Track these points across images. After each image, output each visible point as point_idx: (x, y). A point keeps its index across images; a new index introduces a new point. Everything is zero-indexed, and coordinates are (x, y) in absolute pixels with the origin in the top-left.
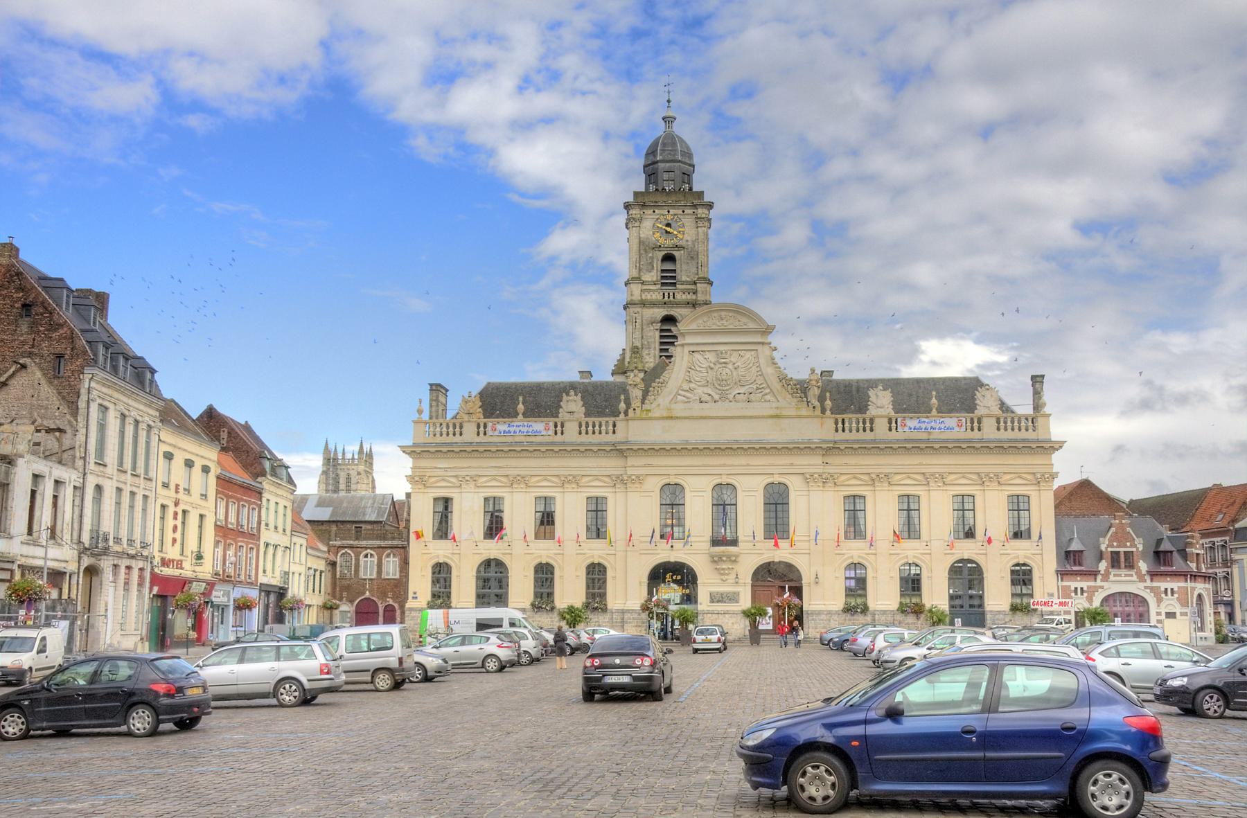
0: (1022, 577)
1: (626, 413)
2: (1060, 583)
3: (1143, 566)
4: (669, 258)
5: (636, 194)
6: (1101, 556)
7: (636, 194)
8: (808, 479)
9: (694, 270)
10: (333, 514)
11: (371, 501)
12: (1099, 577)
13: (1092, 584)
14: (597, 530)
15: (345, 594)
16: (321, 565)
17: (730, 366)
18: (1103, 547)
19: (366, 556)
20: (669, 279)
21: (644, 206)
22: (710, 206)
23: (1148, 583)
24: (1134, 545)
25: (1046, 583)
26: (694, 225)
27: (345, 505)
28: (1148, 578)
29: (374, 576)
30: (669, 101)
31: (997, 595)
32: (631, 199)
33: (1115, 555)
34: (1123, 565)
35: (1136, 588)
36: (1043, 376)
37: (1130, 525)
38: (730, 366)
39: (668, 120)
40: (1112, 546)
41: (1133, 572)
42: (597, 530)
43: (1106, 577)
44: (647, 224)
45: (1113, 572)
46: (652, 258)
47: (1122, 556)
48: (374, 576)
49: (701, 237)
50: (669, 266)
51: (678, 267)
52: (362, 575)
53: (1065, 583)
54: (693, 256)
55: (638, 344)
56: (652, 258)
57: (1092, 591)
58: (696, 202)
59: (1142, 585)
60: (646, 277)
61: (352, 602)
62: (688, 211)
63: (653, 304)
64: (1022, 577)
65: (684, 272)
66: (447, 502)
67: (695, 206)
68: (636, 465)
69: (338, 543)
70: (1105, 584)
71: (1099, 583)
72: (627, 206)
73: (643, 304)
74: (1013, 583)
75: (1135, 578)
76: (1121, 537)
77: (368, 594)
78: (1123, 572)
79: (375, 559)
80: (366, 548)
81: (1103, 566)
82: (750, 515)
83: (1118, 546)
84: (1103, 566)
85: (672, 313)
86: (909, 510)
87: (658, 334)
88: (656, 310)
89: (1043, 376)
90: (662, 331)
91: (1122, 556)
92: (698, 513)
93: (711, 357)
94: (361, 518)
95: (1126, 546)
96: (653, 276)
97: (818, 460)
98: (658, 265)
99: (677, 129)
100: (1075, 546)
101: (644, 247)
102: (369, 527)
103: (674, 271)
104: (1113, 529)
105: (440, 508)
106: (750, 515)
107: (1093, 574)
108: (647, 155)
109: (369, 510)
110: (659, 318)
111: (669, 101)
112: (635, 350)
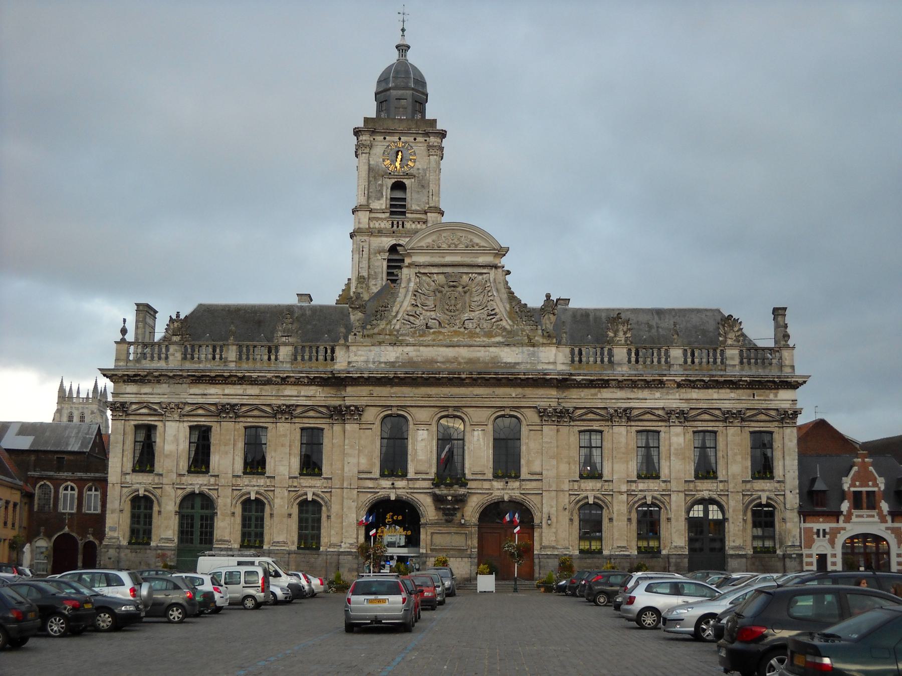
0: (763, 517)
1: (346, 339)
2: (803, 525)
3: (885, 506)
4: (399, 186)
5: (366, 120)
6: (843, 496)
7: (366, 120)
8: (543, 413)
9: (425, 199)
10: (33, 444)
11: (75, 431)
12: (842, 518)
13: (834, 525)
14: (311, 464)
15: (42, 529)
16: (16, 497)
17: (460, 289)
18: (846, 487)
19: (66, 489)
20: (398, 208)
21: (373, 132)
22: (443, 134)
23: (890, 524)
24: (877, 485)
25: (790, 525)
26: (425, 153)
27: (47, 434)
28: (889, 518)
29: (74, 511)
30: (403, 30)
31: (739, 536)
32: (361, 124)
33: (857, 494)
34: (865, 505)
35: (878, 529)
37: (873, 464)
38: (460, 289)
39: (403, 49)
40: (855, 486)
41: (874, 512)
42: (311, 464)
43: (848, 519)
44: (379, 149)
45: (855, 512)
46: (381, 185)
47: (864, 496)
48: (74, 511)
49: (433, 164)
50: (398, 194)
51: (408, 195)
52: (61, 509)
53: (808, 525)
54: (423, 186)
55: (365, 274)
56: (381, 185)
57: (835, 532)
58: (430, 130)
59: (883, 526)
60: (376, 205)
61: (49, 536)
62: (420, 139)
63: (380, 233)
64: (763, 517)
65: (414, 201)
66: (150, 429)
67: (427, 134)
68: (354, 396)
69: (37, 474)
70: (848, 526)
71: (841, 524)
72: (357, 132)
73: (371, 232)
74: (755, 525)
75: (876, 519)
76: (864, 477)
77: (66, 529)
78: (865, 512)
79: (76, 493)
80: (66, 480)
81: (845, 506)
82: (478, 453)
83: (861, 486)
84: (845, 506)
85: (401, 242)
86: (647, 447)
87: (385, 264)
88: (384, 239)
89: (785, 309)
90: (389, 261)
91: (864, 496)
92: (422, 449)
93: (441, 279)
94: (63, 449)
95: (869, 486)
96: (381, 204)
97: (553, 392)
98: (387, 192)
99: (412, 57)
100: (819, 486)
101: (374, 174)
102: (71, 458)
103: (404, 199)
104: (855, 469)
105: (141, 437)
106: (478, 453)
107: (836, 515)
108: (379, 82)
109: (72, 441)
110: (387, 247)
111: (403, 30)
112: (361, 279)
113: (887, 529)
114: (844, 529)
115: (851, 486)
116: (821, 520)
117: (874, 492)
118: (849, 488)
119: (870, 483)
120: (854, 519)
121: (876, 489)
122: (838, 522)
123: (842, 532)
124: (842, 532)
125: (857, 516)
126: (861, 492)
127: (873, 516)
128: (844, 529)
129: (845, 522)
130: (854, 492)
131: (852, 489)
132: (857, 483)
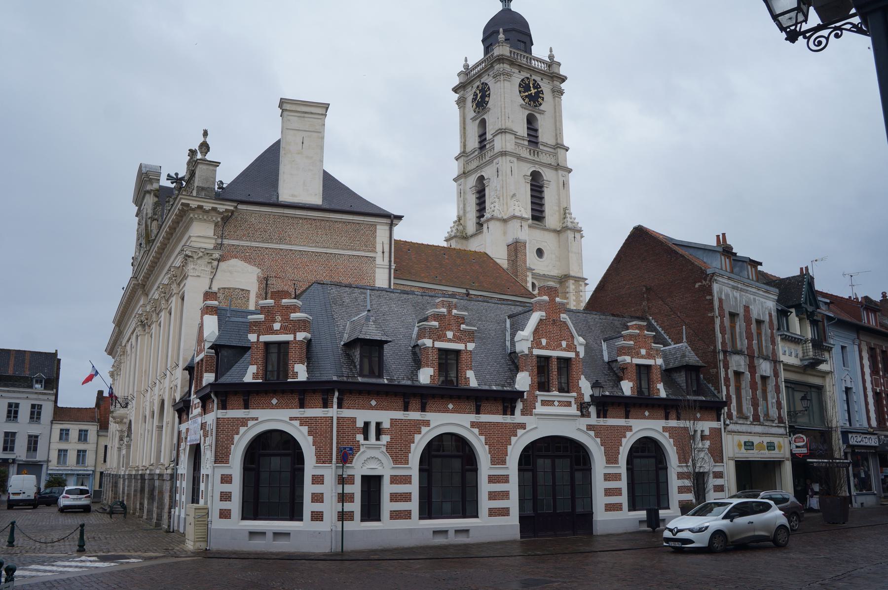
3: (586, 387)
12: (519, 406)
23: (593, 420)
24: (571, 347)
28: (593, 410)
33: (543, 364)
36: (326, 106)
40: (539, 345)
45: (542, 396)
47: (554, 366)
59: (584, 422)
71: (518, 418)
75: (573, 410)
78: (554, 395)
84: (523, 381)
91: (554, 366)
95: (558, 347)
113: (590, 427)
114: (523, 426)
115: (536, 343)
116: (274, 401)
117: (567, 360)
118: (530, 349)
119: (564, 344)
120: (539, 409)
121: (571, 355)
122: (513, 414)
123: (520, 432)
124: (520, 432)
125: (545, 403)
126: (548, 358)
127: (569, 404)
128: (523, 426)
129: (523, 413)
130: (539, 357)
131: (536, 352)
132: (544, 342)
